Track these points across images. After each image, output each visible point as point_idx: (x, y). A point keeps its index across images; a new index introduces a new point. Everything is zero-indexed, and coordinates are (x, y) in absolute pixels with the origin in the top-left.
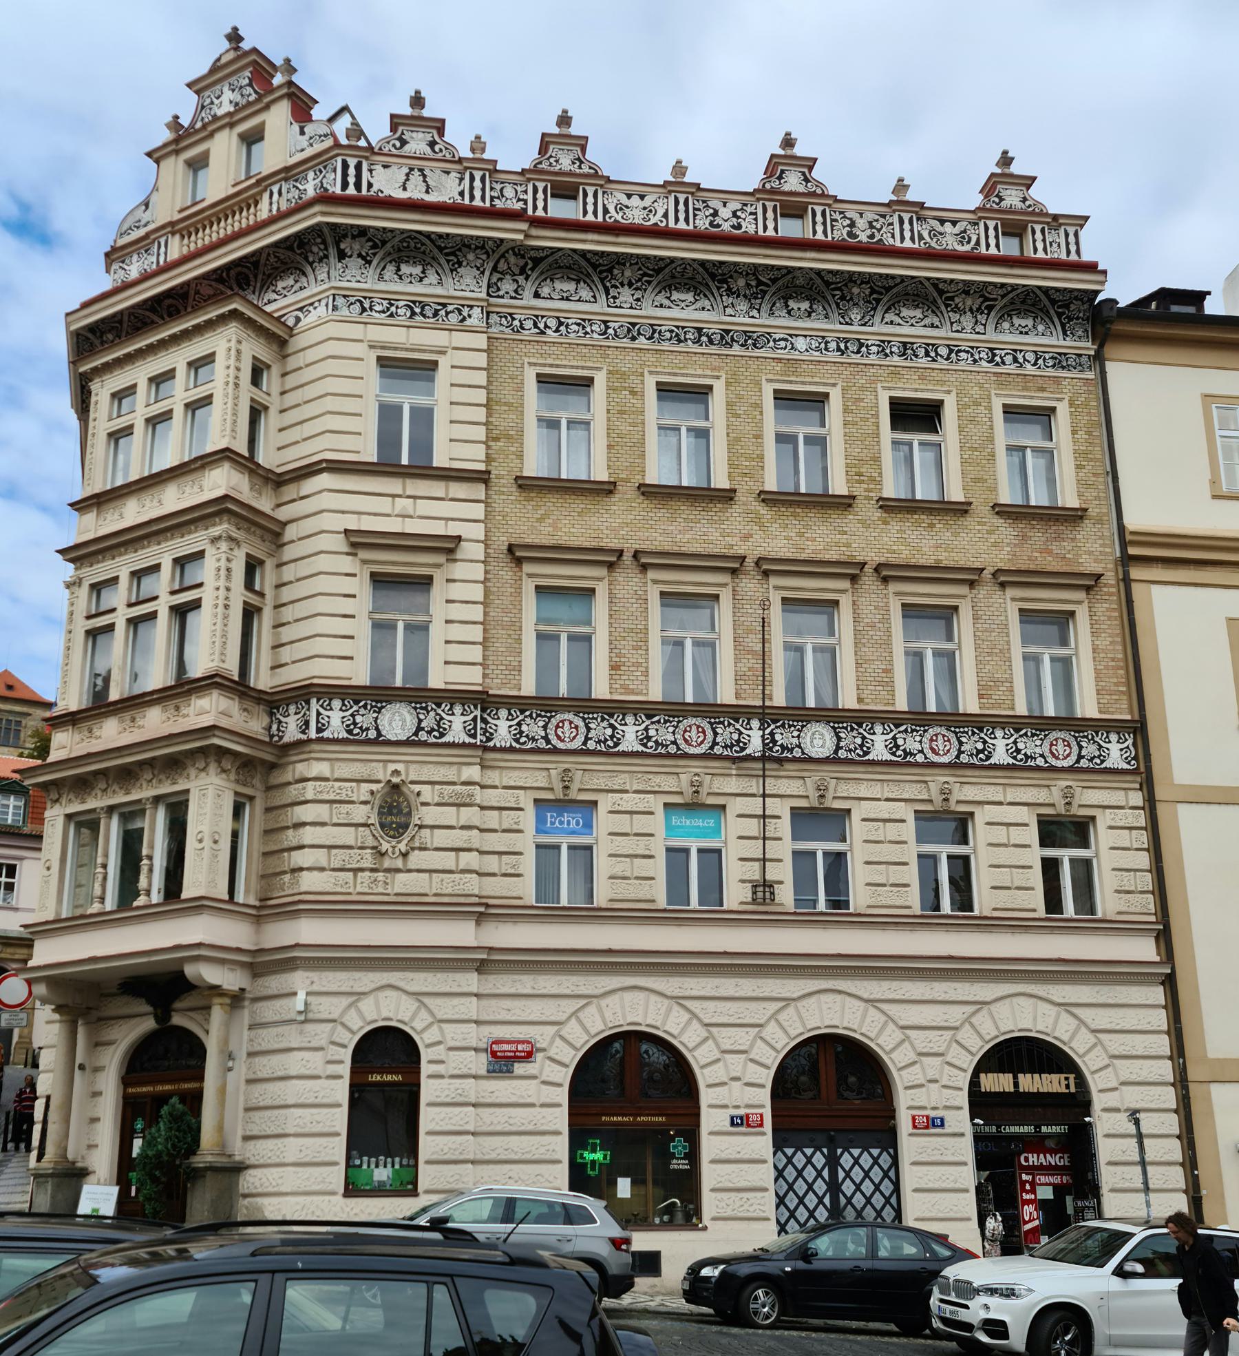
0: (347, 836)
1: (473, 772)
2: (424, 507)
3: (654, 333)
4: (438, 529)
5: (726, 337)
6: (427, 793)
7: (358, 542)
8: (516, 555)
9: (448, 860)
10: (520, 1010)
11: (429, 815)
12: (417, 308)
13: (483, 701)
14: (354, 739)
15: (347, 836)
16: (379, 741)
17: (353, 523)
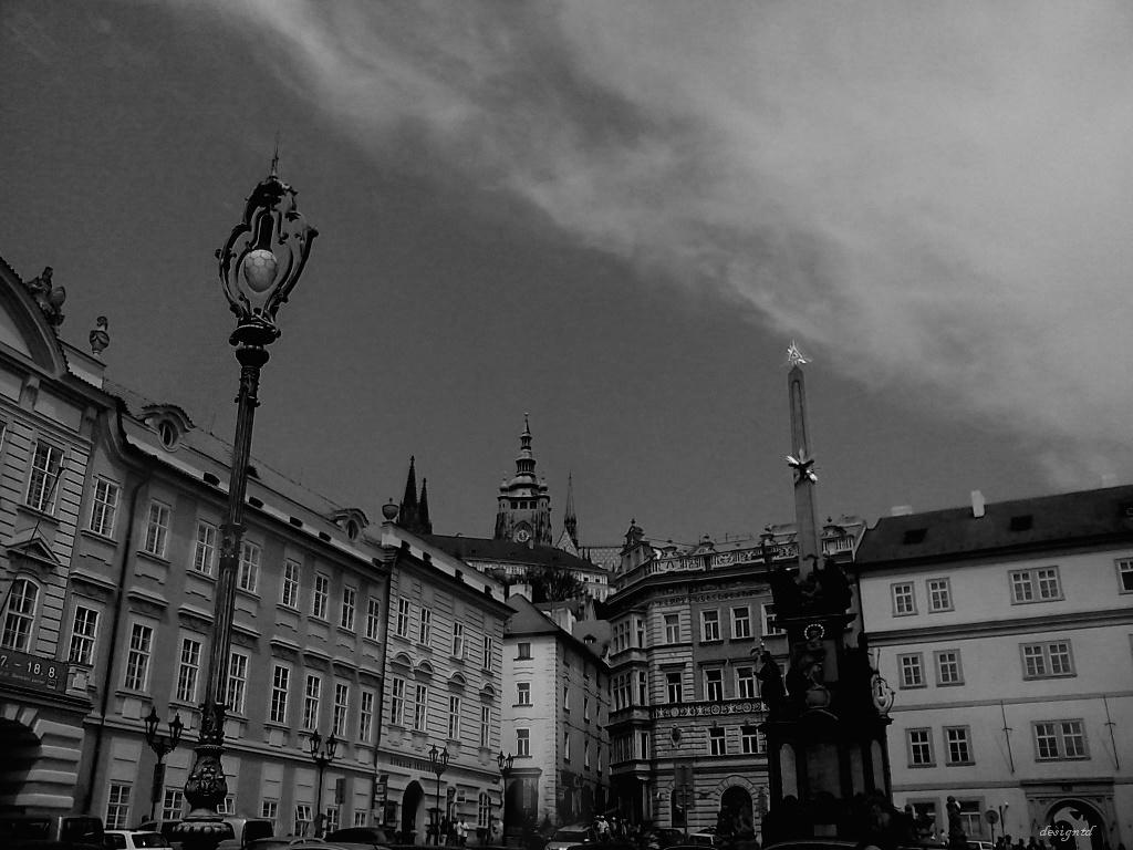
0: (666, 742)
1: (693, 723)
2: (678, 655)
3: (731, 595)
4: (681, 661)
5: (751, 593)
6: (683, 730)
7: (662, 667)
8: (701, 665)
9: (688, 746)
10: (707, 782)
11: (683, 735)
12: (672, 600)
13: (695, 705)
14: (668, 718)
15: (666, 742)
16: (671, 717)
17: (661, 662)
